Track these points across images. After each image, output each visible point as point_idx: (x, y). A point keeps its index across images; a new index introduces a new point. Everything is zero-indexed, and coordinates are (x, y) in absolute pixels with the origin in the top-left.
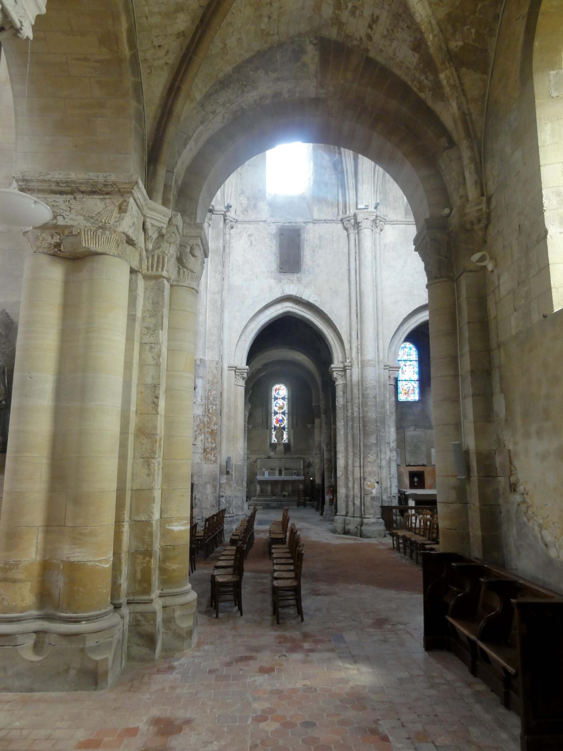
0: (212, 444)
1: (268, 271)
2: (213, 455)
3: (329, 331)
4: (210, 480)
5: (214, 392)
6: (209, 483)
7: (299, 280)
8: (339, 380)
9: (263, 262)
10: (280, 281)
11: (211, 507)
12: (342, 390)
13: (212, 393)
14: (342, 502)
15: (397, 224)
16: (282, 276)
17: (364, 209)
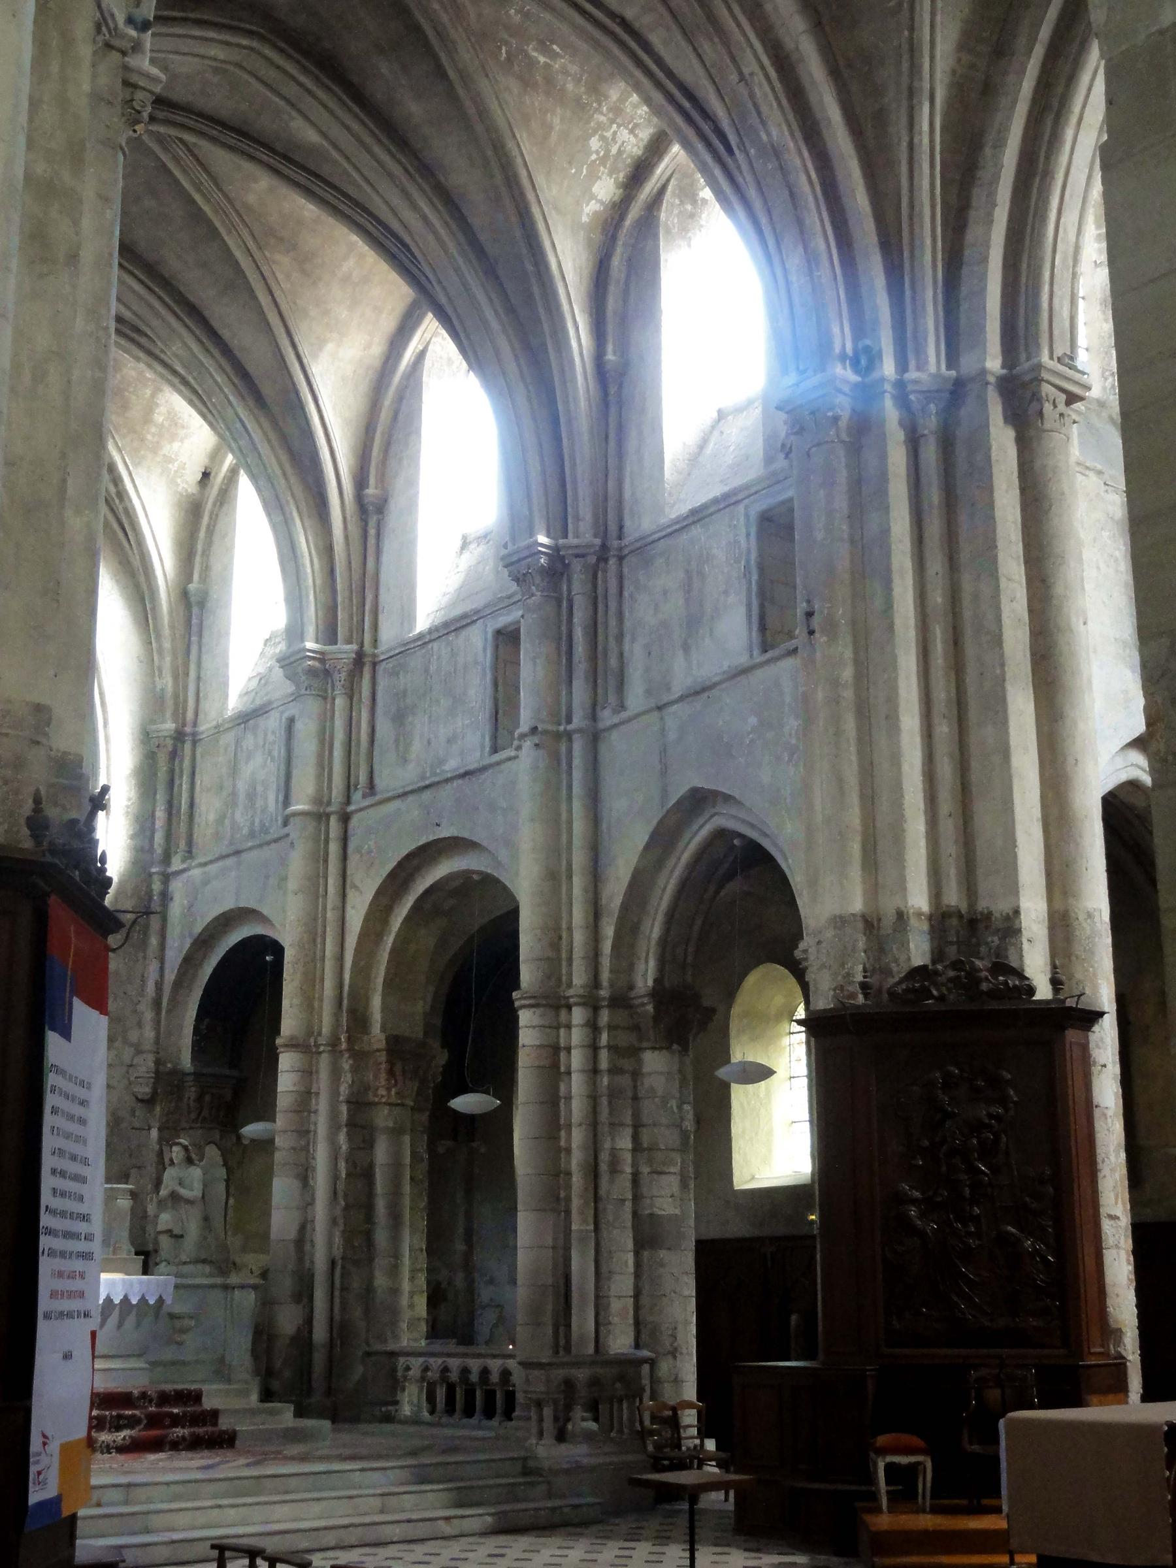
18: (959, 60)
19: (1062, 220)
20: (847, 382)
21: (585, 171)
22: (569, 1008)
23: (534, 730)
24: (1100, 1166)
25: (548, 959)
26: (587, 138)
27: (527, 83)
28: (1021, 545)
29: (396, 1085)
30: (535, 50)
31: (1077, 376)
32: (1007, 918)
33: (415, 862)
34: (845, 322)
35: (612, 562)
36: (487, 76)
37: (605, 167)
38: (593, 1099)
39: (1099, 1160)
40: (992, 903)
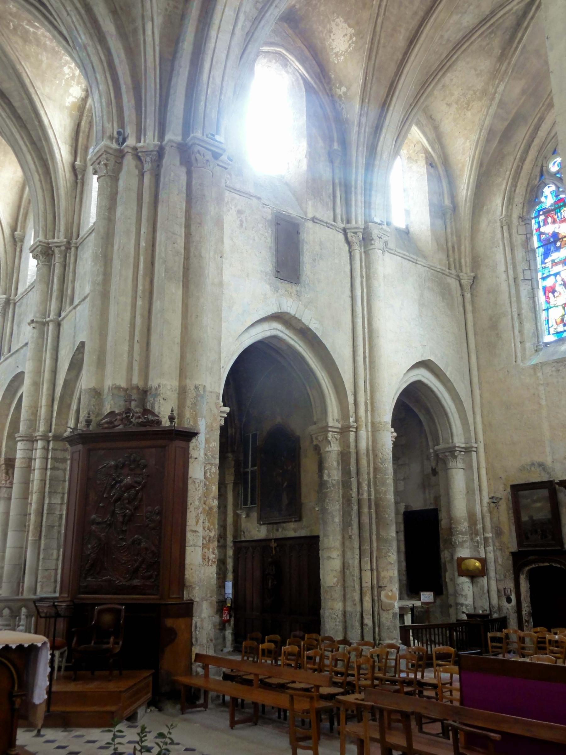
0: (210, 531)
1: (262, 271)
2: (211, 550)
3: (323, 374)
4: (206, 595)
5: (213, 443)
6: (206, 600)
7: (298, 295)
8: (332, 445)
9: (256, 255)
10: (276, 290)
11: (208, 642)
12: (336, 459)
13: (211, 446)
14: (337, 623)
15: (395, 254)
16: (278, 283)
17: (379, 224)
18: (168, 4)
19: (212, 73)
20: (111, 148)
21: (64, 82)
22: (37, 441)
23: (32, 321)
24: (189, 506)
25: (30, 420)
26: (62, 67)
27: (26, 39)
28: (184, 219)
29: (9, 478)
30: (27, 25)
31: (216, 144)
32: (156, 389)
33: (16, 384)
34: (114, 122)
35: (73, 249)
36: (3, 35)
37: (74, 81)
38: (43, 481)
39: (189, 503)
40: (153, 383)
